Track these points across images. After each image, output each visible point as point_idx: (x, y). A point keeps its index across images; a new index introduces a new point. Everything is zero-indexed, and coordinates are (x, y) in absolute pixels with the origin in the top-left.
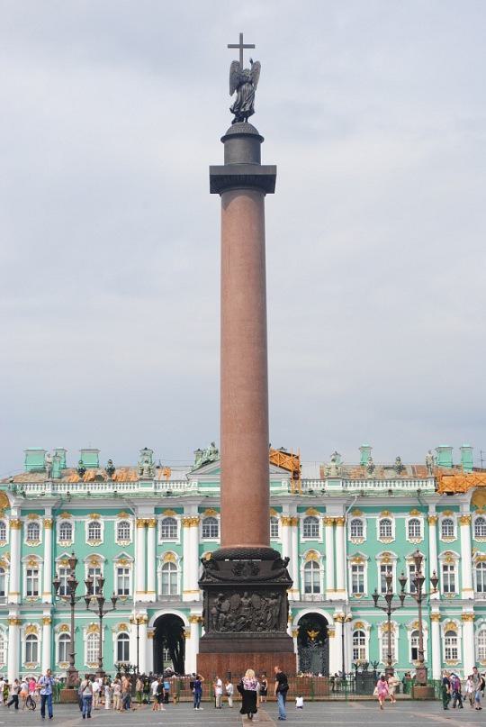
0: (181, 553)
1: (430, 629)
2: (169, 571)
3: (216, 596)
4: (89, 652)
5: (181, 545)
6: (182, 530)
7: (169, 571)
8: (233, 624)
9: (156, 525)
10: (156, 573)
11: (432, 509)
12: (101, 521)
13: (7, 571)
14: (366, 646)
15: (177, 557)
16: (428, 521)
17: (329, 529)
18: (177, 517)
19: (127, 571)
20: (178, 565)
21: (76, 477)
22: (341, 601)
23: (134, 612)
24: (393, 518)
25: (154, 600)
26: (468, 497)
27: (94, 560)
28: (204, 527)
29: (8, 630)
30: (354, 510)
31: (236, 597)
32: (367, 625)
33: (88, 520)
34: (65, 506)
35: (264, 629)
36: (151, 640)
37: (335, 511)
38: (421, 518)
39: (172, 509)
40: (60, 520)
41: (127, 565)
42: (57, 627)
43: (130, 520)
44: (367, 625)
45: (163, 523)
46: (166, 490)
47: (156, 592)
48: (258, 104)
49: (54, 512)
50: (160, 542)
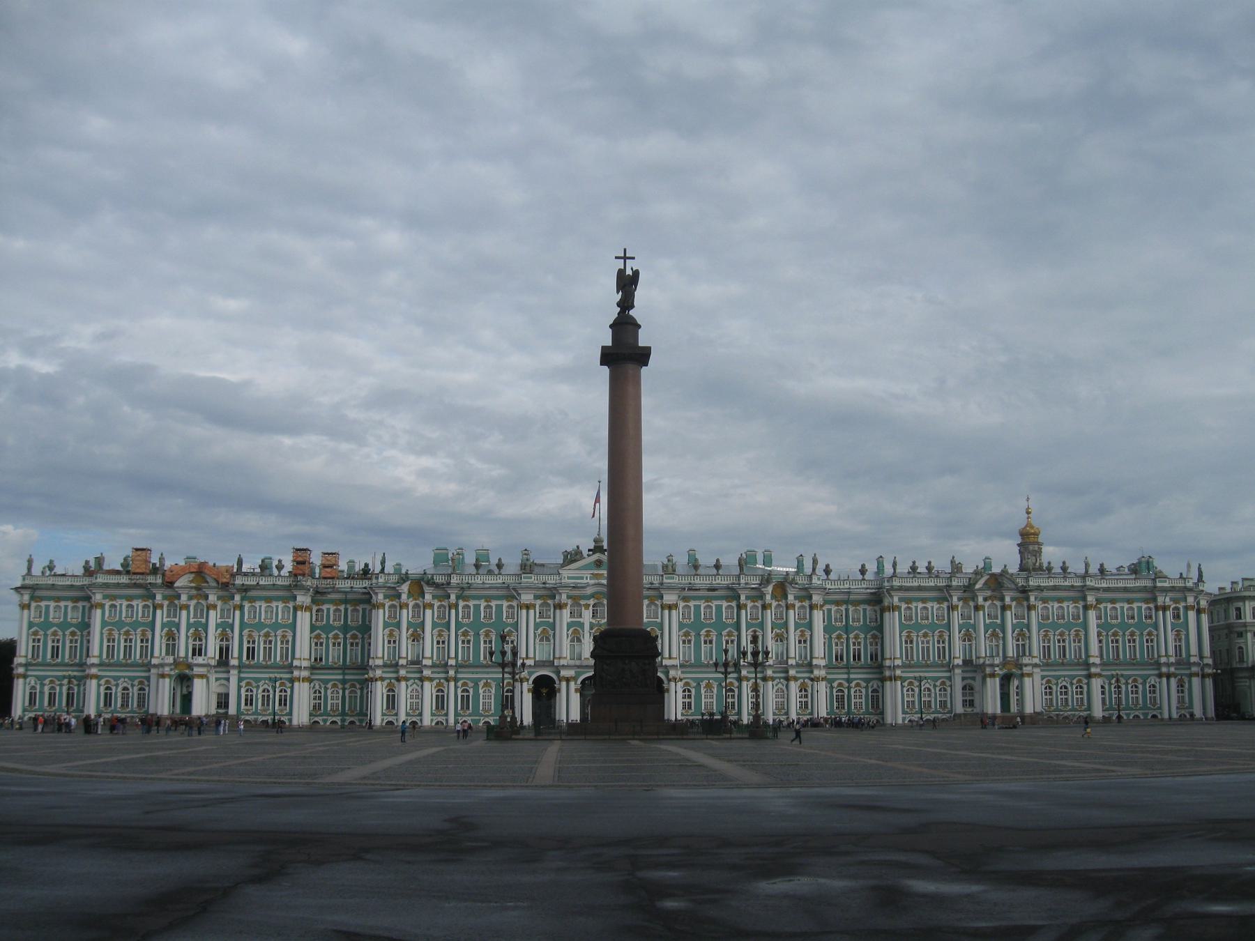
0: (554, 629)
1: (740, 688)
9: (534, 606)
11: (743, 598)
15: (551, 633)
16: (739, 607)
17: (666, 612)
18: (550, 602)
22: (674, 667)
24: (714, 604)
26: (770, 589)
27: (487, 635)
30: (685, 599)
33: (483, 604)
34: (467, 593)
37: (669, 598)
38: (734, 604)
40: (461, 603)
42: (459, 684)
43: (514, 603)
49: (458, 598)
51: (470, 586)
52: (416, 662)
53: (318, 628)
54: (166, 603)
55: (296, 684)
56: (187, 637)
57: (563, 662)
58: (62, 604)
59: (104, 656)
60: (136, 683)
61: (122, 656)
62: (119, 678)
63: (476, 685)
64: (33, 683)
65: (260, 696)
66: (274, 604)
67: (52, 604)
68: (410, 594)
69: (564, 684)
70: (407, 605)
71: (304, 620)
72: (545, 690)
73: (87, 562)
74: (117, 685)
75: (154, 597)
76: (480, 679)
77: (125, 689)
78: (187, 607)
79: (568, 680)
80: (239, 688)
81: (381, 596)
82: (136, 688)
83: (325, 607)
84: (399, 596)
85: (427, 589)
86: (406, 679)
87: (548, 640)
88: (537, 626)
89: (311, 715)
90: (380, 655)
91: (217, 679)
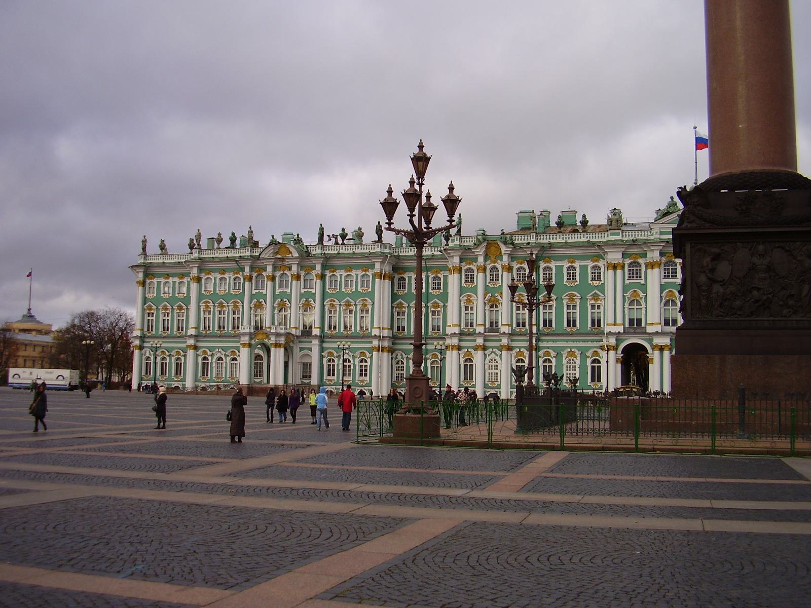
0: (645, 291)
2: (635, 307)
5: (645, 285)
6: (646, 273)
7: (635, 307)
8: (738, 303)
9: (623, 267)
10: (624, 308)
12: (577, 265)
13: (500, 307)
18: (641, 261)
19: (599, 307)
20: (643, 302)
23: (604, 340)
25: (622, 331)
27: (572, 299)
28: (665, 269)
33: (566, 264)
36: (619, 365)
39: (636, 254)
41: (599, 302)
42: (541, 353)
43: (601, 264)
45: (629, 267)
46: (631, 238)
47: (624, 324)
50: (627, 282)
51: (551, 246)
52: (493, 327)
53: (400, 297)
54: (255, 275)
55: (375, 354)
56: (274, 308)
57: (658, 328)
58: (171, 280)
59: (202, 328)
60: (228, 353)
61: (216, 328)
62: (215, 348)
63: (558, 356)
64: (148, 355)
65: (341, 367)
66: (353, 273)
67: (163, 280)
68: (486, 257)
69: (657, 353)
70: (484, 270)
71: (382, 290)
72: (634, 360)
73: (192, 240)
74: (212, 355)
75: (243, 270)
76: (564, 348)
77: (220, 359)
78: (273, 279)
79: (661, 349)
80: (322, 357)
81: (456, 260)
82: (228, 359)
83: (406, 276)
84: (476, 260)
85: (503, 248)
86: (484, 348)
87: (639, 303)
88: (625, 288)
89: (393, 385)
90: (456, 322)
91: (301, 349)
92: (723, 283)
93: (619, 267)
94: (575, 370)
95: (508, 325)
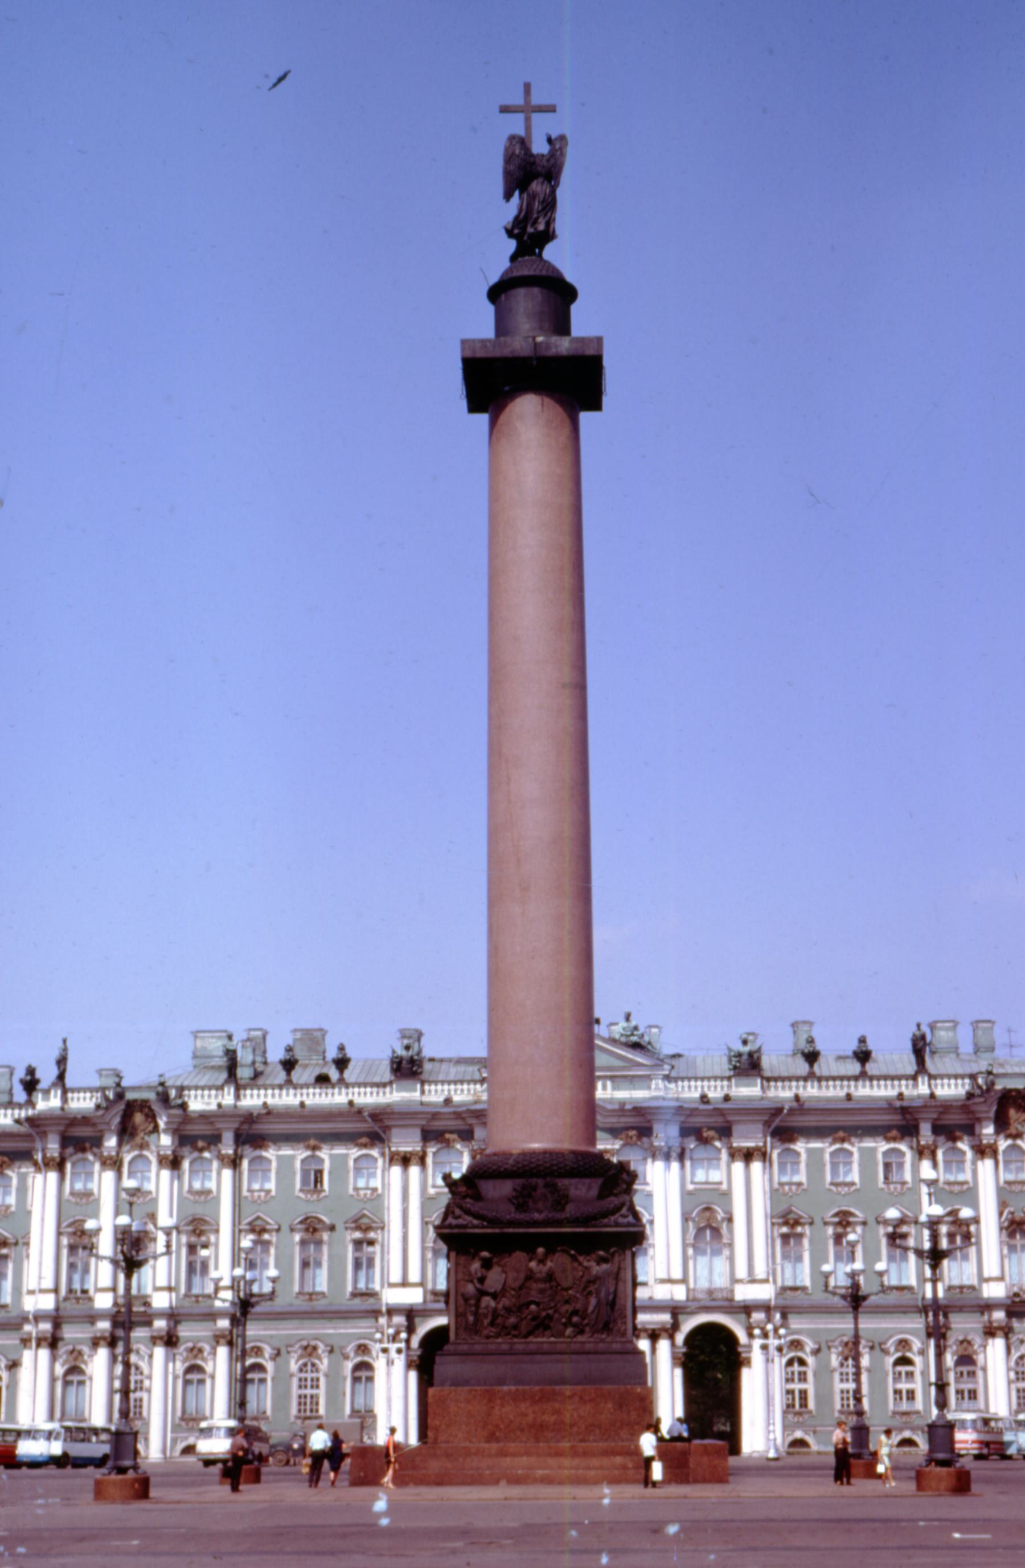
3: (474, 1256)
4: (300, 1397)
8: (512, 1320)
14: (810, 1386)
21: (281, 1076)
29: (151, 1356)
31: (519, 1256)
32: (809, 1345)
35: (581, 1332)
44: (809, 1345)
48: (564, 220)
92: (494, 1296)
93: (414, 1160)
94: (318, 1387)
95: (170, 1289)
